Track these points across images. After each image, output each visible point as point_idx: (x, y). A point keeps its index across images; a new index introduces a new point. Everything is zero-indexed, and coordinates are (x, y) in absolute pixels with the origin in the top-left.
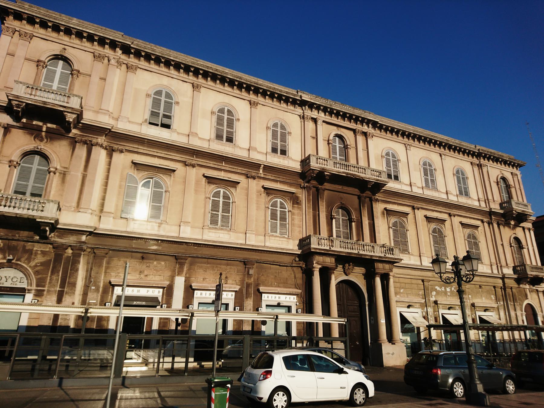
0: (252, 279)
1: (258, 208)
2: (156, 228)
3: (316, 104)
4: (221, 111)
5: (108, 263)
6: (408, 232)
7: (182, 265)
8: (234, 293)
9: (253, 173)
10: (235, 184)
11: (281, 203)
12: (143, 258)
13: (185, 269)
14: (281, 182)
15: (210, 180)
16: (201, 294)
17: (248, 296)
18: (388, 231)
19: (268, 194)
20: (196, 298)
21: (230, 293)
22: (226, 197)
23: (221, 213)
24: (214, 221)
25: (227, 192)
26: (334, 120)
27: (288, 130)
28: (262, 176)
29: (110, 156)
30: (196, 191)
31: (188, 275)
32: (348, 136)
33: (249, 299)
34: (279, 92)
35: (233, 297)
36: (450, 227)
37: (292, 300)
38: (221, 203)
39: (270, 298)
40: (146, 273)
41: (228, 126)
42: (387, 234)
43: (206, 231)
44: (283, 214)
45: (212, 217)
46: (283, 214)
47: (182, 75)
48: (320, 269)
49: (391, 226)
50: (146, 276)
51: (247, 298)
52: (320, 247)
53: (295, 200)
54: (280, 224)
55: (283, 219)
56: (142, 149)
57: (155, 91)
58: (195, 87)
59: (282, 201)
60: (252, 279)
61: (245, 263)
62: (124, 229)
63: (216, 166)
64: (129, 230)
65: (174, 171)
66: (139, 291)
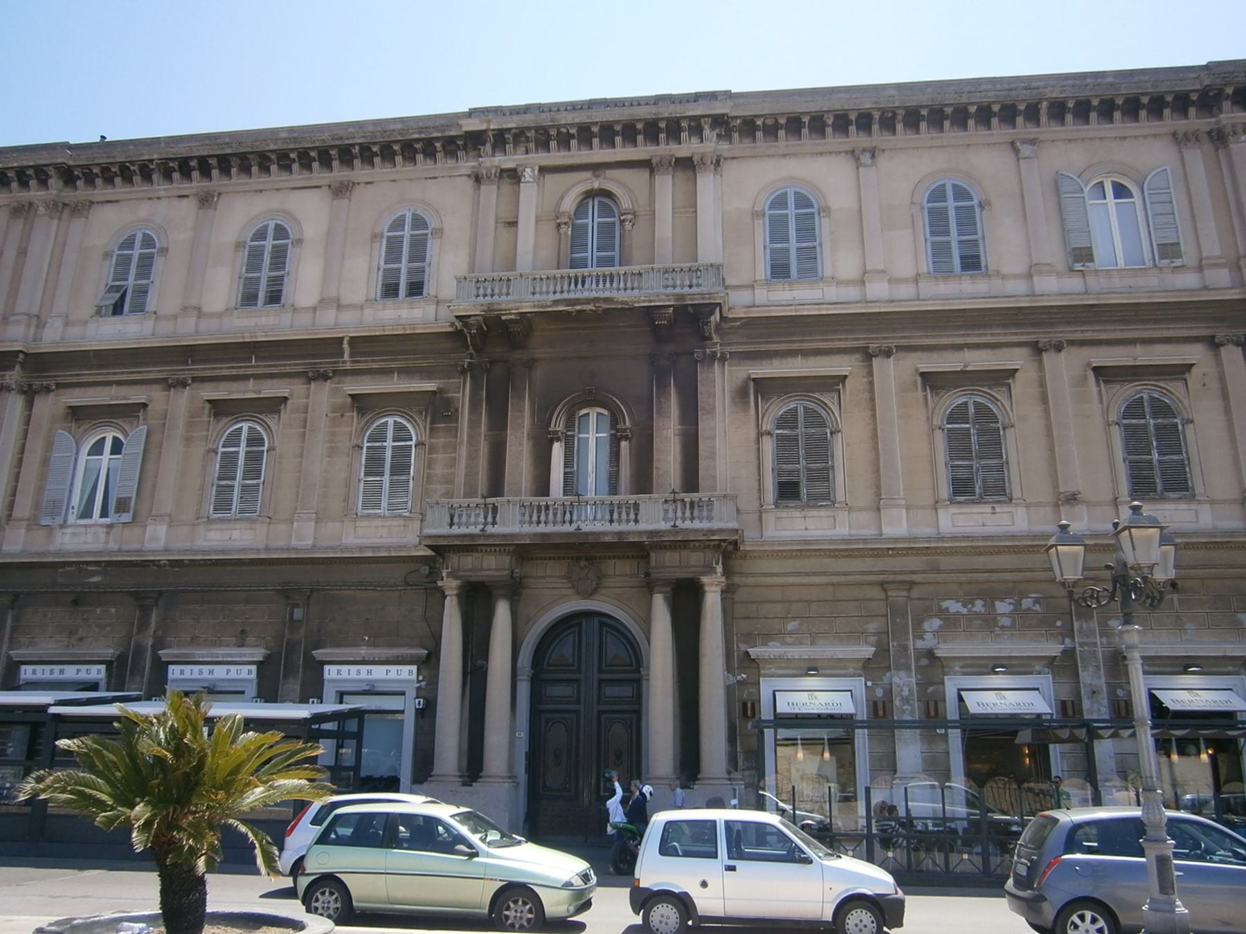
0: (302, 631)
1: (332, 452)
2: (102, 537)
3: (509, 130)
4: (780, 202)
5: (16, 619)
6: (1009, 432)
7: (145, 612)
8: (254, 668)
9: (325, 364)
10: (275, 405)
11: (399, 428)
12: (76, 602)
13: (154, 619)
14: (405, 372)
15: (220, 409)
16: (339, 672)
17: (290, 671)
18: (754, 446)
19: (362, 411)
20: (173, 681)
21: (246, 668)
22: (255, 440)
23: (976, 468)
24: (223, 504)
25: (258, 428)
26: (556, 157)
27: (433, 224)
28: (348, 366)
29: (30, 405)
30: (188, 440)
31: (160, 633)
32: (612, 181)
33: (291, 680)
34: (338, 143)
35: (254, 676)
36: (1034, 390)
37: (244, 675)
38: (242, 456)
39: (344, 675)
40: (81, 633)
41: (139, 276)
42: (752, 457)
43: (942, 514)
44: (401, 455)
45: (218, 493)
46: (401, 455)
47: (299, 176)
48: (460, 588)
49: (767, 425)
50: (81, 639)
51: (285, 677)
52: (455, 530)
53: (438, 410)
54: (391, 482)
55: (400, 467)
56: (87, 375)
57: (121, 241)
58: (206, 201)
59: (399, 420)
60: (302, 631)
61: (138, 596)
62: (187, 545)
63: (234, 372)
64: (52, 548)
65: (145, 405)
66: (62, 672)
